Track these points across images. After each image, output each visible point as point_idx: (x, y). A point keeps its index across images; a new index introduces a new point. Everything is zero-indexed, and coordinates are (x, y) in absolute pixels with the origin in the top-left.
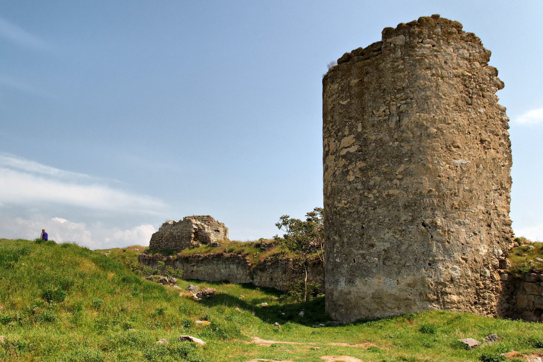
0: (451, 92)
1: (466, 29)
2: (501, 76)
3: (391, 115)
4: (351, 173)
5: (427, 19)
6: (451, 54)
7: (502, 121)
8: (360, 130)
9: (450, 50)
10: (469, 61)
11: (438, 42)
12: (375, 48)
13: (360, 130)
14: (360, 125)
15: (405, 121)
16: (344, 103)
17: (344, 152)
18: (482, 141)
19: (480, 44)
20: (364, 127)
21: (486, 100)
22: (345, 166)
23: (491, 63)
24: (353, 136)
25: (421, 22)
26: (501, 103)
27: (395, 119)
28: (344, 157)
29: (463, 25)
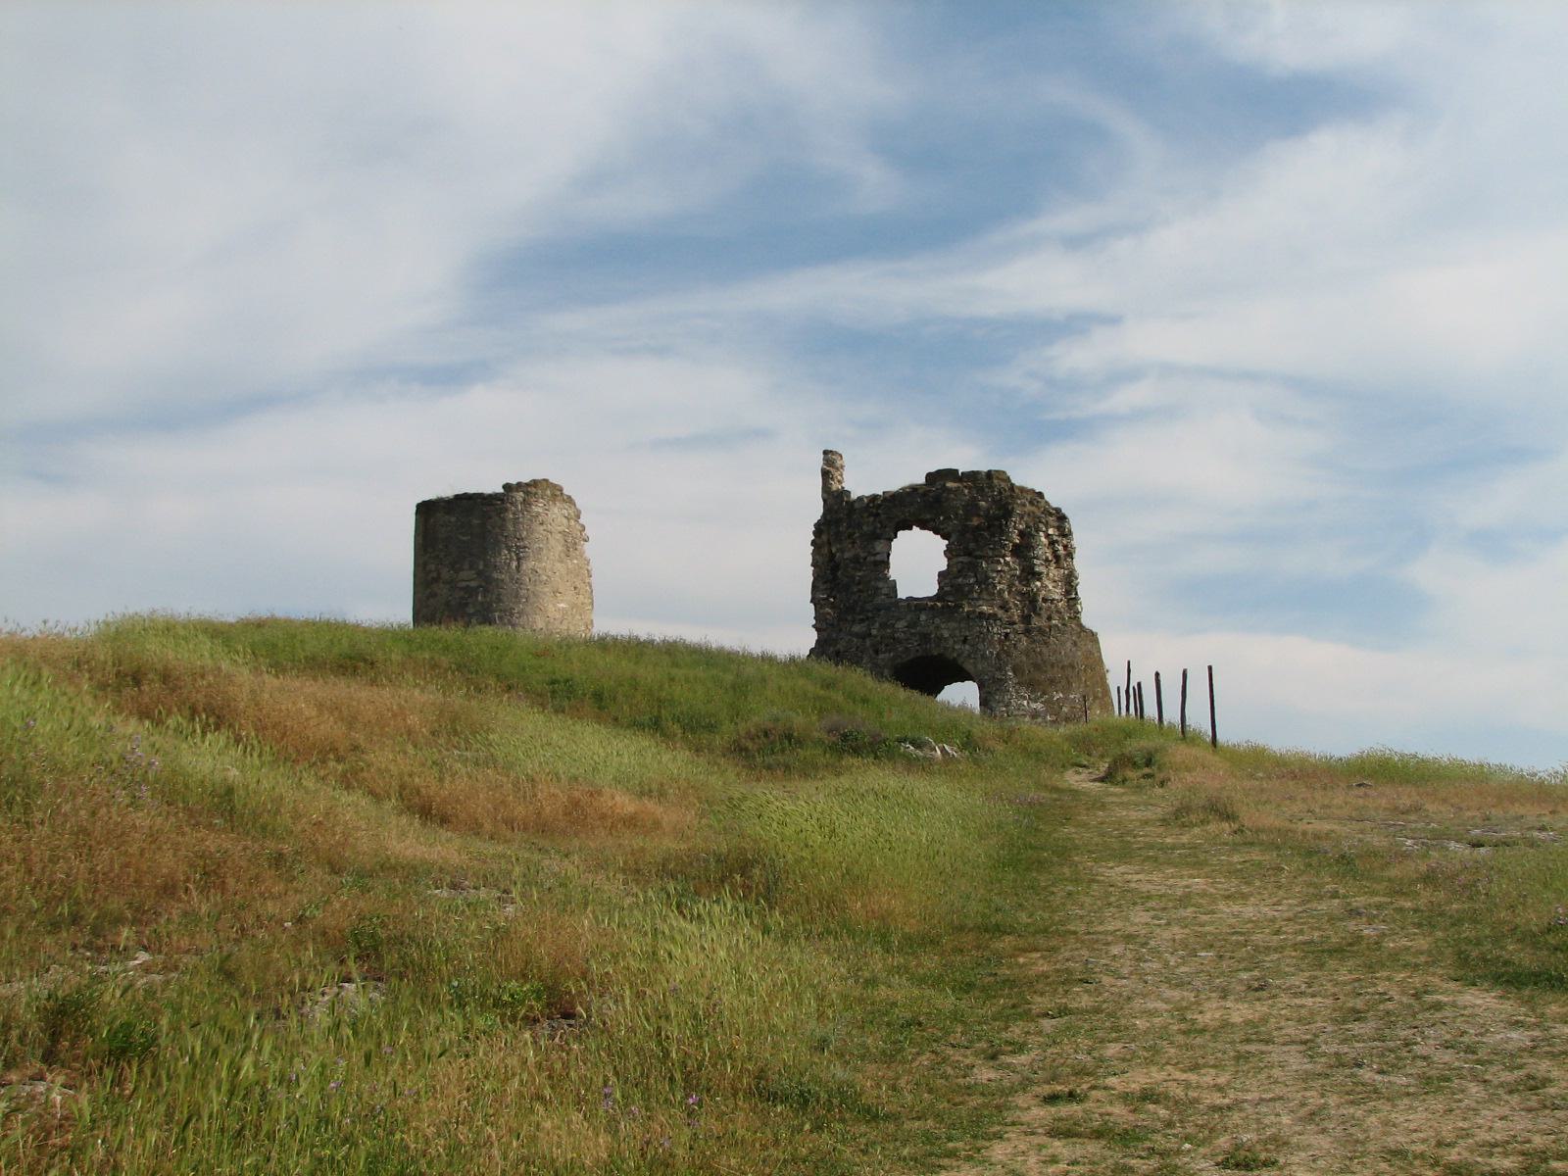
0: (557, 546)
1: (565, 492)
2: (588, 532)
3: (511, 559)
4: (471, 606)
5: (539, 481)
6: (557, 512)
7: (588, 570)
8: (481, 567)
9: (556, 510)
10: (568, 519)
11: (548, 503)
12: (494, 497)
13: (481, 567)
14: (482, 563)
15: (524, 567)
16: (465, 538)
17: (464, 584)
18: (575, 588)
19: (575, 506)
20: (485, 565)
21: (578, 553)
22: (462, 598)
23: (581, 521)
24: (473, 572)
25: (535, 483)
26: (588, 554)
27: (514, 564)
28: (461, 589)
29: (563, 485)
